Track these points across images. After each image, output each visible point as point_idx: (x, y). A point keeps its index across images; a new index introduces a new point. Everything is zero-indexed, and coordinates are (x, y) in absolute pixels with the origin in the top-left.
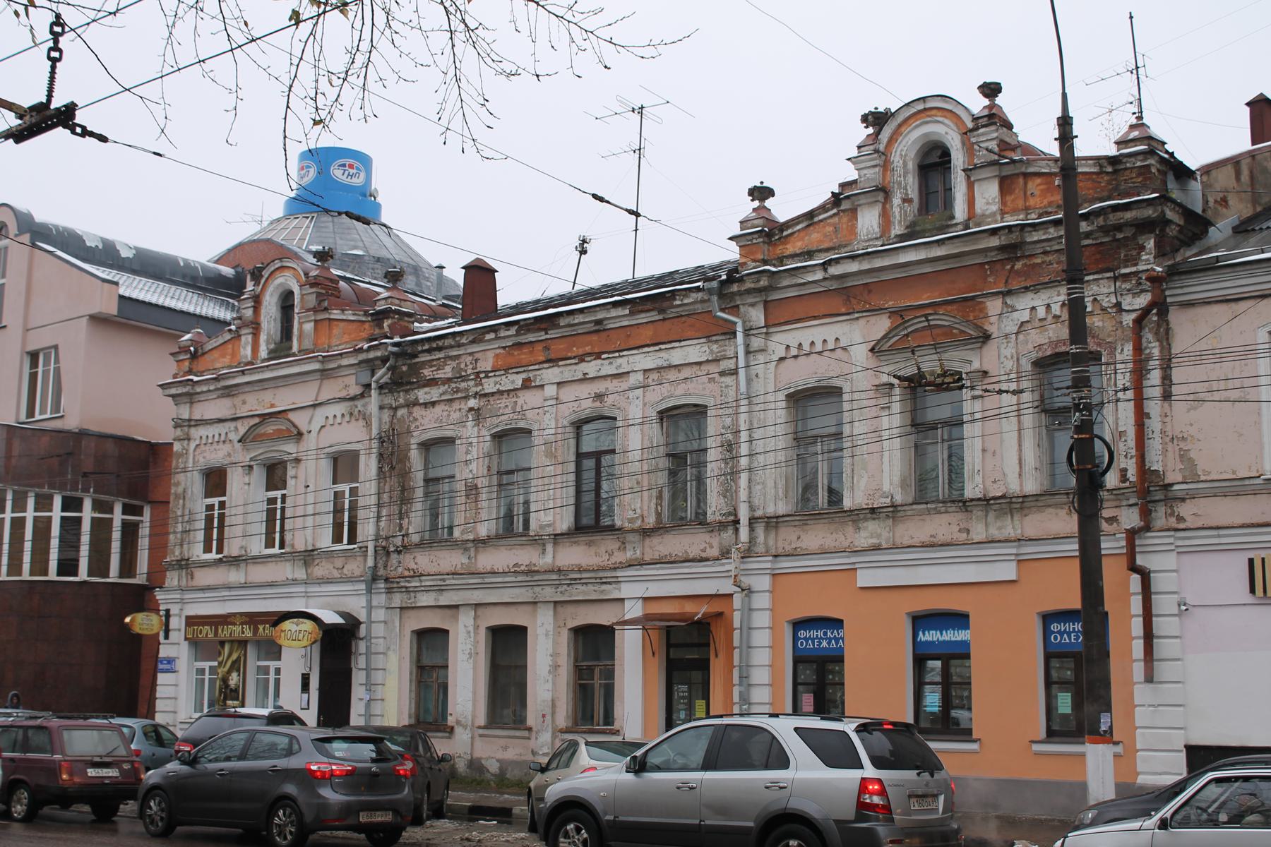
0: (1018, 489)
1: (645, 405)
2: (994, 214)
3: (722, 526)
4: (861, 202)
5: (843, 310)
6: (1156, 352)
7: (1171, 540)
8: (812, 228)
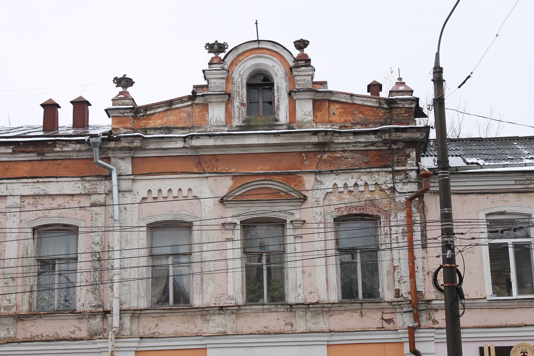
0: (326, 298)
1: (21, 221)
2: (309, 122)
3: (93, 315)
4: (212, 100)
5: (195, 170)
6: (418, 219)
7: (433, 335)
8: (169, 112)
